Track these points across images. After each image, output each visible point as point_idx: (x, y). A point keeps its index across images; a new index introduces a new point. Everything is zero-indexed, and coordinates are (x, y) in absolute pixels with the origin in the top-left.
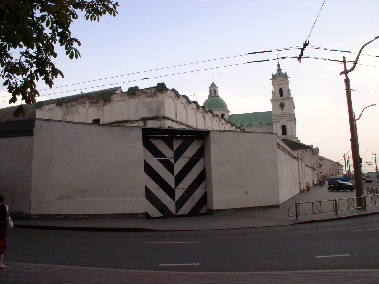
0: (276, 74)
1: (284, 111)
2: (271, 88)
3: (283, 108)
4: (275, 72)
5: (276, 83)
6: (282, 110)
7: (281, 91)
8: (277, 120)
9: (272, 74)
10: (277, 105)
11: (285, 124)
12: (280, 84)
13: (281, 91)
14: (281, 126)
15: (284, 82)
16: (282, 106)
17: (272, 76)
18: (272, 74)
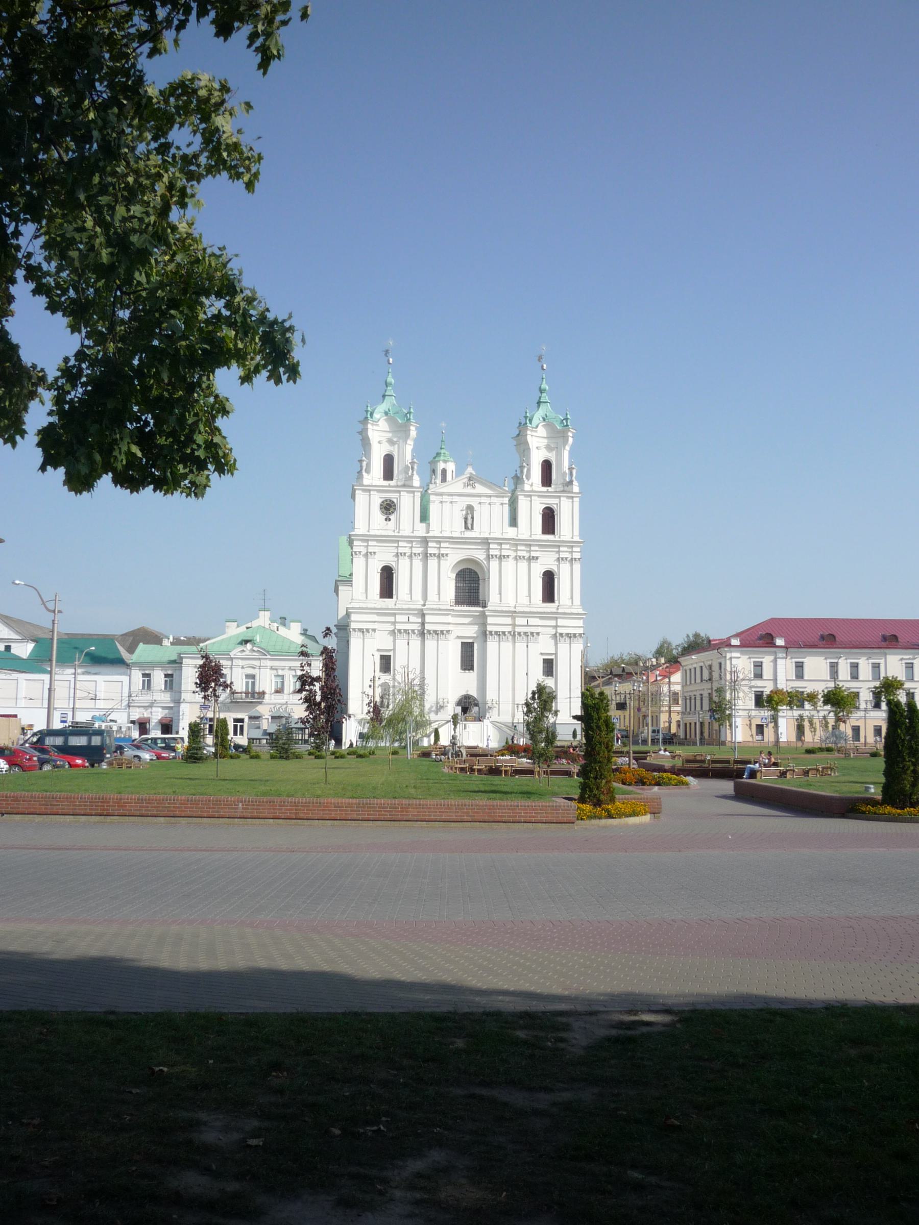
1: (392, 524)
3: (390, 514)
11: (393, 565)
14: (379, 571)
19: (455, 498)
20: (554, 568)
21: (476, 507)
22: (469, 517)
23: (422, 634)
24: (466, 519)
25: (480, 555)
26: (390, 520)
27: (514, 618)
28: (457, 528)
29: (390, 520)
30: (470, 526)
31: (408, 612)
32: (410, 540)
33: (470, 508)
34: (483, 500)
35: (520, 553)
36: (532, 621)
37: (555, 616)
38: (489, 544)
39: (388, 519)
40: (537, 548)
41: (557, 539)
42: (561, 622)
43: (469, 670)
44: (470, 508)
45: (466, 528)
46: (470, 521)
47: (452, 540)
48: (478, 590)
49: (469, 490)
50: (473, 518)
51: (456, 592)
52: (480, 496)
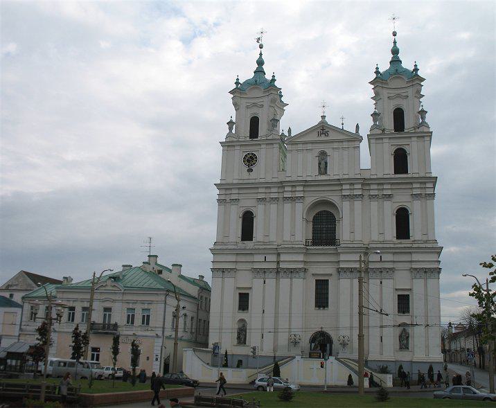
0: (247, 83)
2: (230, 113)
4: (247, 74)
5: (243, 103)
6: (250, 170)
7: (254, 122)
8: (233, 197)
9: (238, 79)
10: (239, 155)
11: (253, 210)
12: (255, 105)
13: (254, 122)
15: (266, 99)
16: (250, 160)
17: (237, 83)
18: (238, 79)
19: (309, 146)
20: (408, 206)
21: (329, 152)
22: (323, 162)
23: (278, 272)
24: (320, 164)
25: (335, 199)
26: (251, 170)
27: (366, 254)
28: (311, 172)
29: (251, 170)
30: (322, 170)
31: (265, 252)
32: (268, 185)
33: (323, 154)
34: (335, 145)
35: (372, 193)
36: (386, 257)
37: (409, 251)
38: (341, 185)
39: (250, 170)
40: (389, 187)
41: (409, 176)
42: (415, 257)
43: (324, 307)
44: (323, 154)
45: (320, 173)
46: (323, 166)
47: (306, 184)
48: (335, 230)
49: (323, 138)
50: (326, 163)
51: (313, 233)
52: (332, 142)
